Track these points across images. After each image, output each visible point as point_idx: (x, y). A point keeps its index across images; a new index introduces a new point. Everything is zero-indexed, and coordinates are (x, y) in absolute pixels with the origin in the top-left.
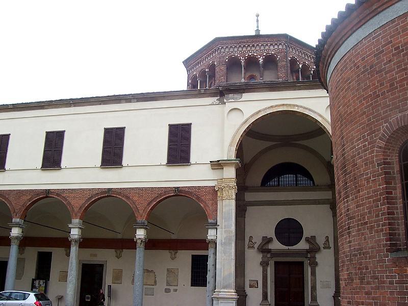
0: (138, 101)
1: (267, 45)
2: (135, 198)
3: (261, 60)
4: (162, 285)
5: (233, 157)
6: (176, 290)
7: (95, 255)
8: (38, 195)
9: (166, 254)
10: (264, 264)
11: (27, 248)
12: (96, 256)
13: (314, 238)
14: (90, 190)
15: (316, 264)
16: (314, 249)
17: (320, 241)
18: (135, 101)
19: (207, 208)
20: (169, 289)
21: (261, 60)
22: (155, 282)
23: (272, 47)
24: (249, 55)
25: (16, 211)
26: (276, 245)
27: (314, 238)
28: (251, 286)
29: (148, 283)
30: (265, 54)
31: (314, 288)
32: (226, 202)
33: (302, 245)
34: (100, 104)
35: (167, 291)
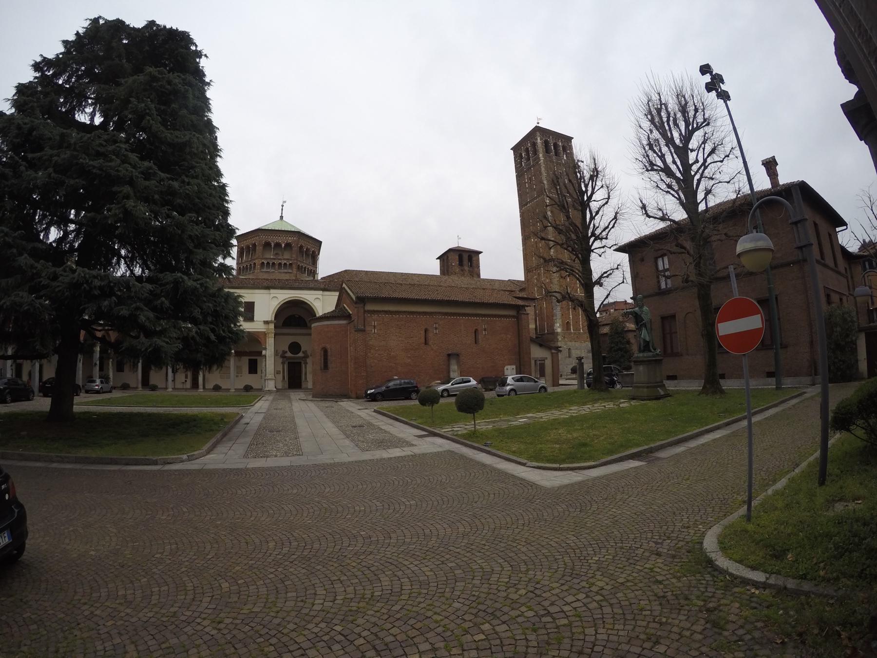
3: (283, 245)
6: (241, 376)
10: (283, 363)
13: (306, 351)
15: (307, 363)
16: (306, 356)
17: (309, 353)
21: (283, 245)
26: (289, 354)
27: (306, 351)
31: (306, 374)
33: (301, 354)
35: (237, 376)
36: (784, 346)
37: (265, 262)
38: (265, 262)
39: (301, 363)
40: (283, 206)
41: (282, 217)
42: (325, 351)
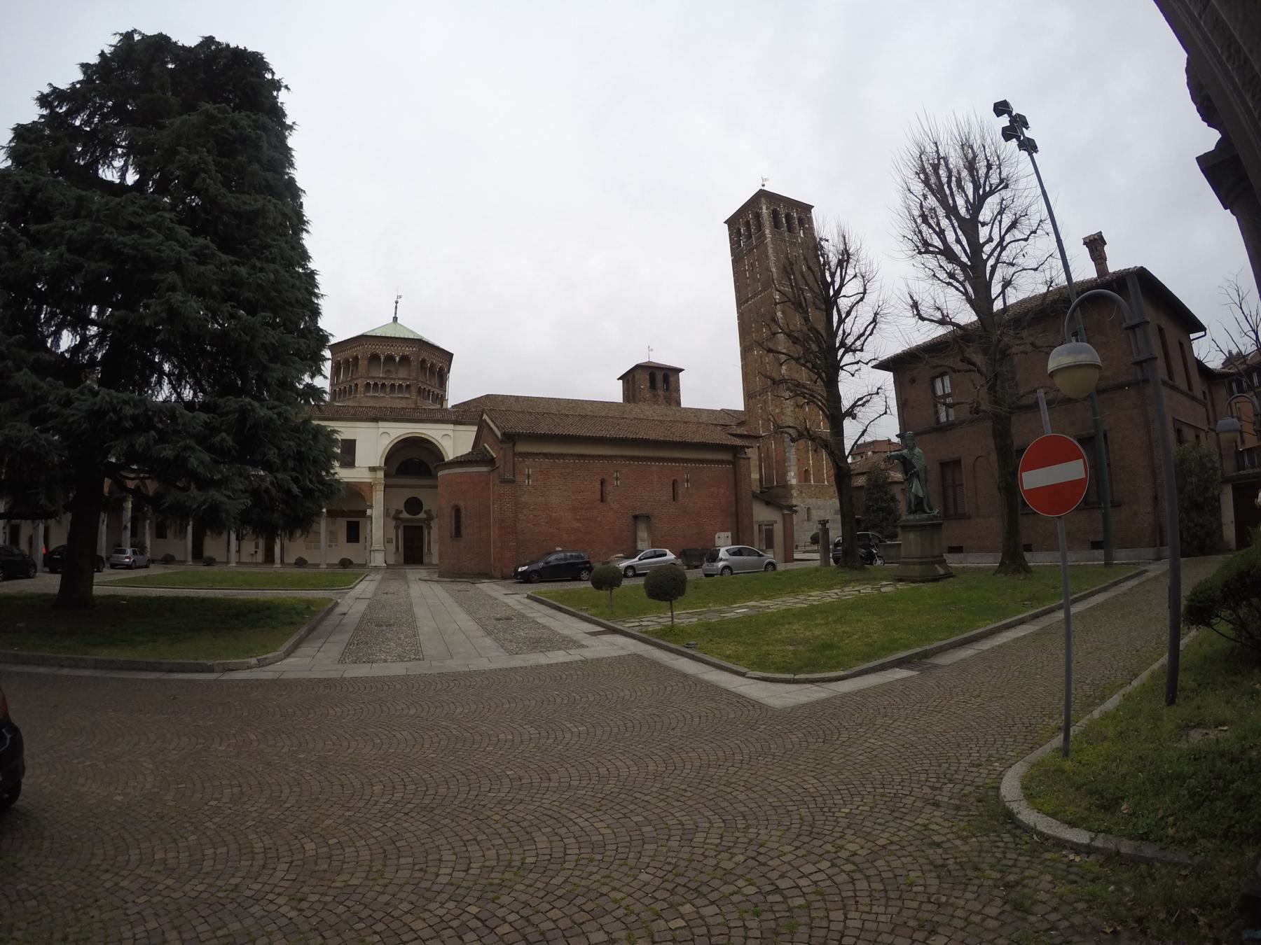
3: (397, 359)
5: (383, 465)
6: (336, 546)
10: (397, 528)
15: (431, 528)
17: (434, 513)
21: (397, 359)
26: (405, 515)
27: (430, 510)
31: (429, 543)
32: (378, 493)
33: (422, 515)
35: (330, 546)
36: (1117, 505)
37: (372, 383)
38: (372, 383)
39: (421, 528)
40: (397, 302)
41: (395, 319)
42: (457, 511)
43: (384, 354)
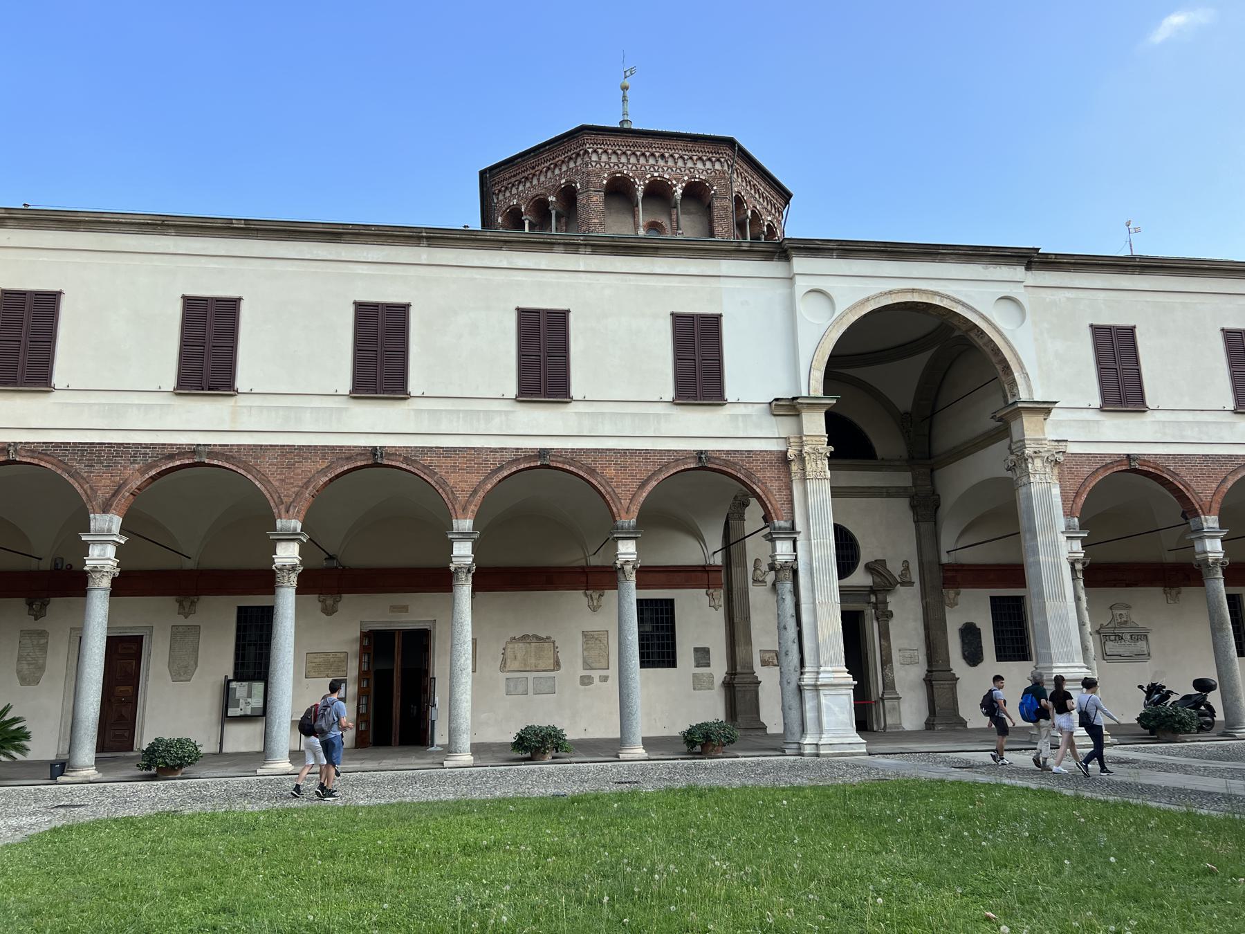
0: (593, 253)
1: (691, 158)
2: (610, 472)
4: (573, 666)
7: (405, 609)
8: (349, 459)
9: (577, 598)
11: (202, 598)
12: (407, 611)
13: (882, 562)
14: (494, 450)
17: (895, 568)
18: (589, 250)
19: (770, 496)
20: (590, 677)
22: (557, 665)
23: (699, 165)
24: (653, 176)
25: (285, 499)
28: (764, 663)
29: (541, 666)
30: (686, 178)
34: (500, 249)
35: (586, 681)
40: (625, 88)
43: (642, 177)
